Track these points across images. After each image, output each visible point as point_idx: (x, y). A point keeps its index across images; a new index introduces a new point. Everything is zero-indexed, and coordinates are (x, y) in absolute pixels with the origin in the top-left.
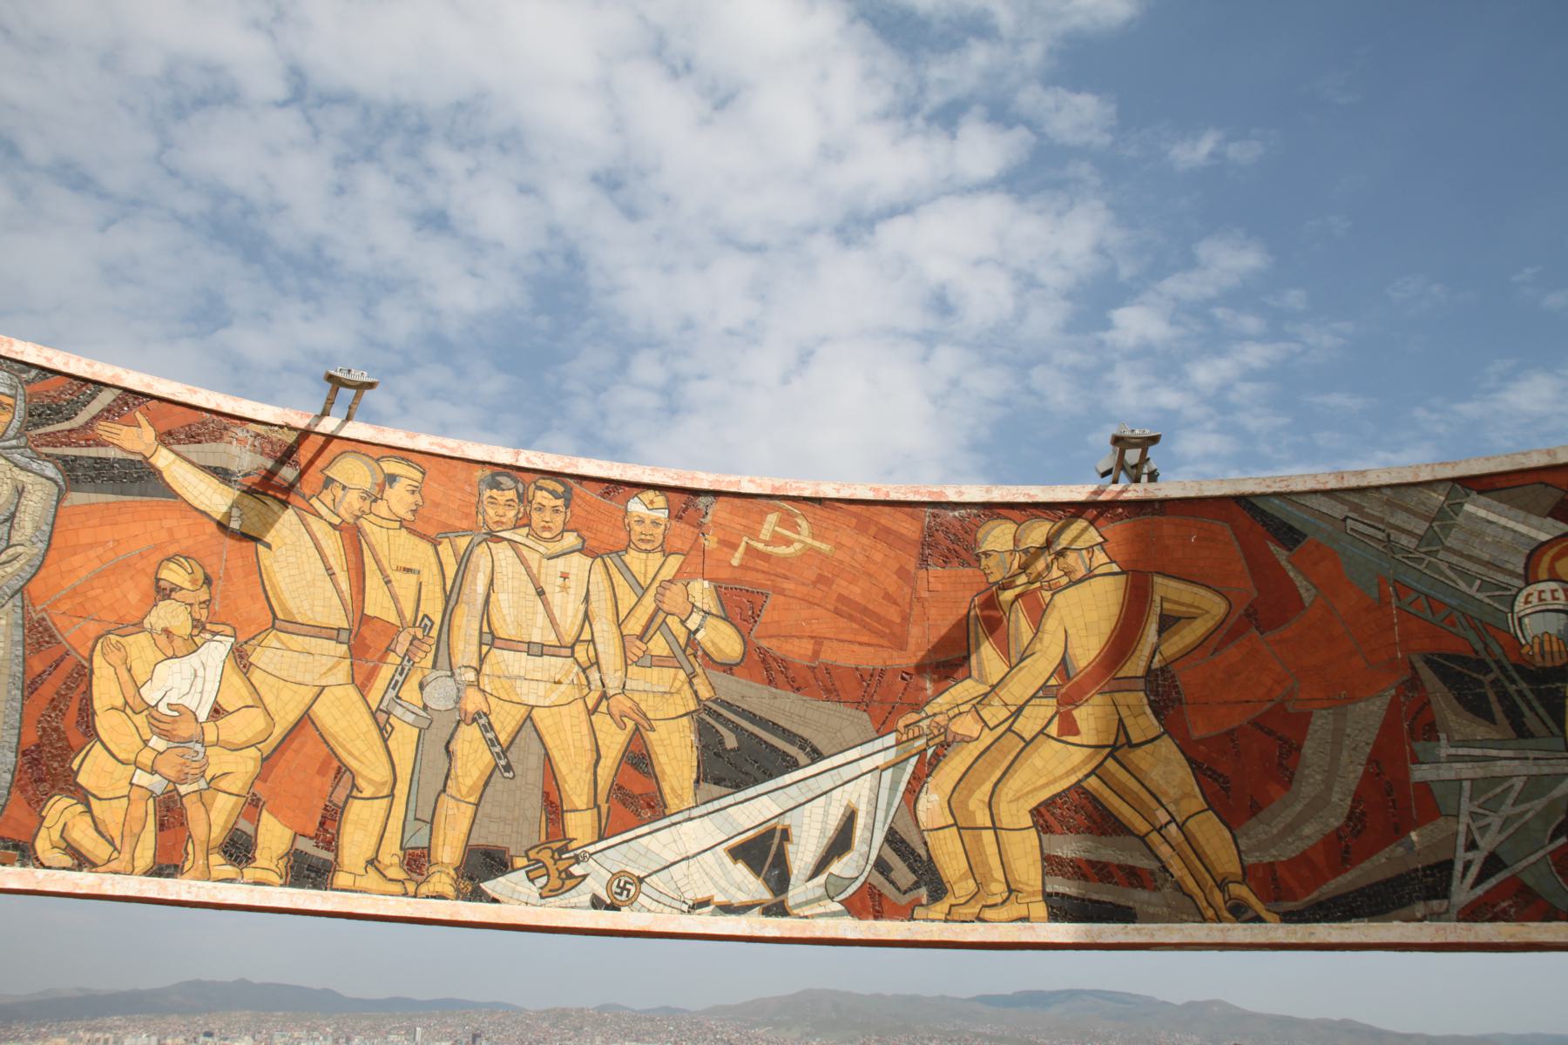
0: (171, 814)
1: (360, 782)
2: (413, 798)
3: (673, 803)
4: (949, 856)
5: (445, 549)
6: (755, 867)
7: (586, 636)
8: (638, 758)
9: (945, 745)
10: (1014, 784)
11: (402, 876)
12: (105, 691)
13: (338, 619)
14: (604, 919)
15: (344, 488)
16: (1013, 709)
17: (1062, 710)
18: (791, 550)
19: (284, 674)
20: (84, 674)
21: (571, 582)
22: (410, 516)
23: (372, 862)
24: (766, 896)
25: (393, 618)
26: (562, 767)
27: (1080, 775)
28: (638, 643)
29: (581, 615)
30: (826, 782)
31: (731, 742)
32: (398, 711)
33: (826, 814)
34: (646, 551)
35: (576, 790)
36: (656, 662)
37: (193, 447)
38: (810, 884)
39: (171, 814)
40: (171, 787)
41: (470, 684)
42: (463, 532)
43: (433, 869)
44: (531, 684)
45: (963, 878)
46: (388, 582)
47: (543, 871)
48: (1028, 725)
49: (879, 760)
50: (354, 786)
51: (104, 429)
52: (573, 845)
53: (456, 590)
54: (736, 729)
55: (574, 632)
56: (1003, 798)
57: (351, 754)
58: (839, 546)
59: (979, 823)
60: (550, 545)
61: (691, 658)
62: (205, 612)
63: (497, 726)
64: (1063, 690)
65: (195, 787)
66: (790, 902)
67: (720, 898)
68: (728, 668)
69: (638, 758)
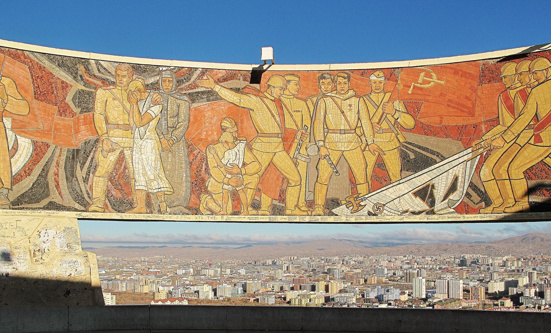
0: (235, 196)
1: (290, 181)
2: (307, 184)
3: (393, 179)
4: (492, 191)
5: (309, 102)
6: (423, 199)
7: (359, 125)
8: (380, 164)
9: (490, 150)
10: (517, 162)
11: (306, 209)
12: (212, 163)
13: (277, 130)
14: (374, 219)
15: (274, 87)
16: (516, 135)
17: (536, 133)
18: (430, 85)
19: (263, 150)
20: (205, 159)
21: (352, 108)
22: (296, 93)
23: (297, 206)
24: (427, 208)
25: (295, 128)
26: (355, 170)
27: (543, 158)
28: (378, 125)
29: (357, 118)
30: (446, 167)
31: (412, 156)
32: (300, 158)
33: (447, 179)
34: (378, 93)
35: (360, 177)
36: (385, 131)
37: (225, 83)
38: (442, 203)
39: (235, 196)
40: (234, 188)
41: (322, 146)
42: (313, 96)
43: (316, 207)
44: (343, 143)
45: (498, 197)
46: (292, 116)
47: (351, 204)
48: (522, 141)
49: (466, 158)
50: (288, 183)
51: (198, 82)
52: (360, 195)
53: (314, 115)
54: (413, 151)
55: (355, 125)
56: (513, 168)
57: (286, 173)
58: (447, 81)
59: (504, 178)
60: (344, 96)
61: (396, 128)
62: (236, 134)
63: (332, 159)
64: (536, 126)
65: (241, 188)
66: (436, 210)
67: (411, 210)
68: (410, 130)
69: (380, 164)
